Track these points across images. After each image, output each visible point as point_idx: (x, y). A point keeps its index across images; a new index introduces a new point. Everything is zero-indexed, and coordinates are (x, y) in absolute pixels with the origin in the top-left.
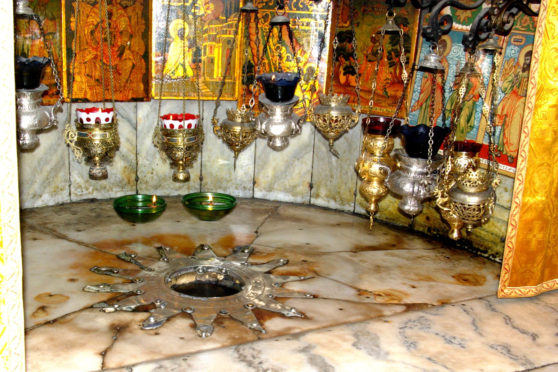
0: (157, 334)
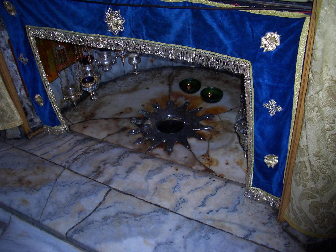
0: (128, 136)
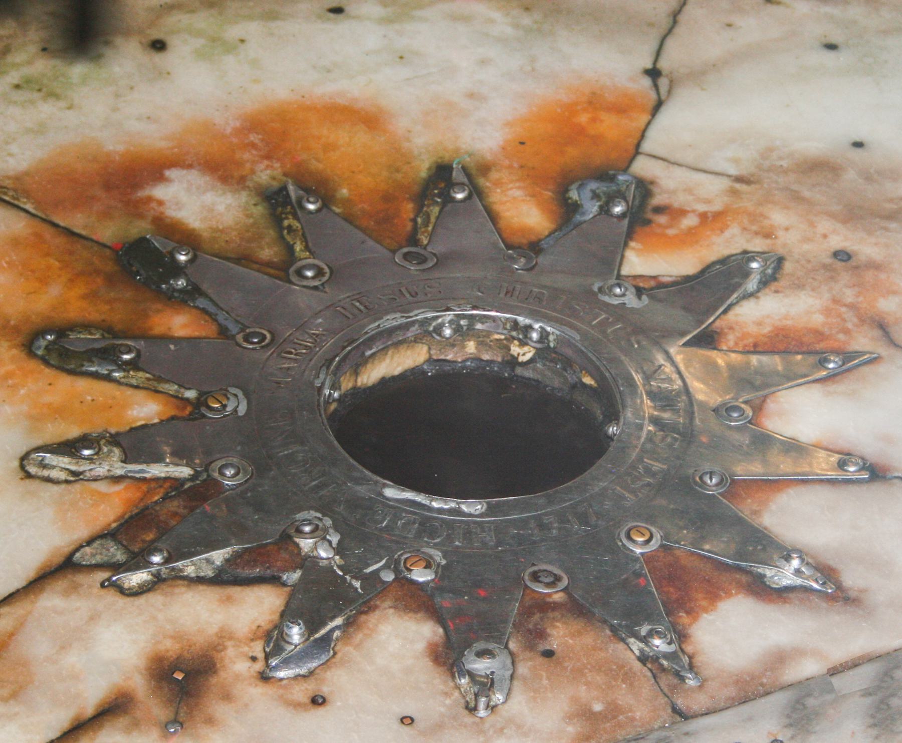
0: (318, 701)
